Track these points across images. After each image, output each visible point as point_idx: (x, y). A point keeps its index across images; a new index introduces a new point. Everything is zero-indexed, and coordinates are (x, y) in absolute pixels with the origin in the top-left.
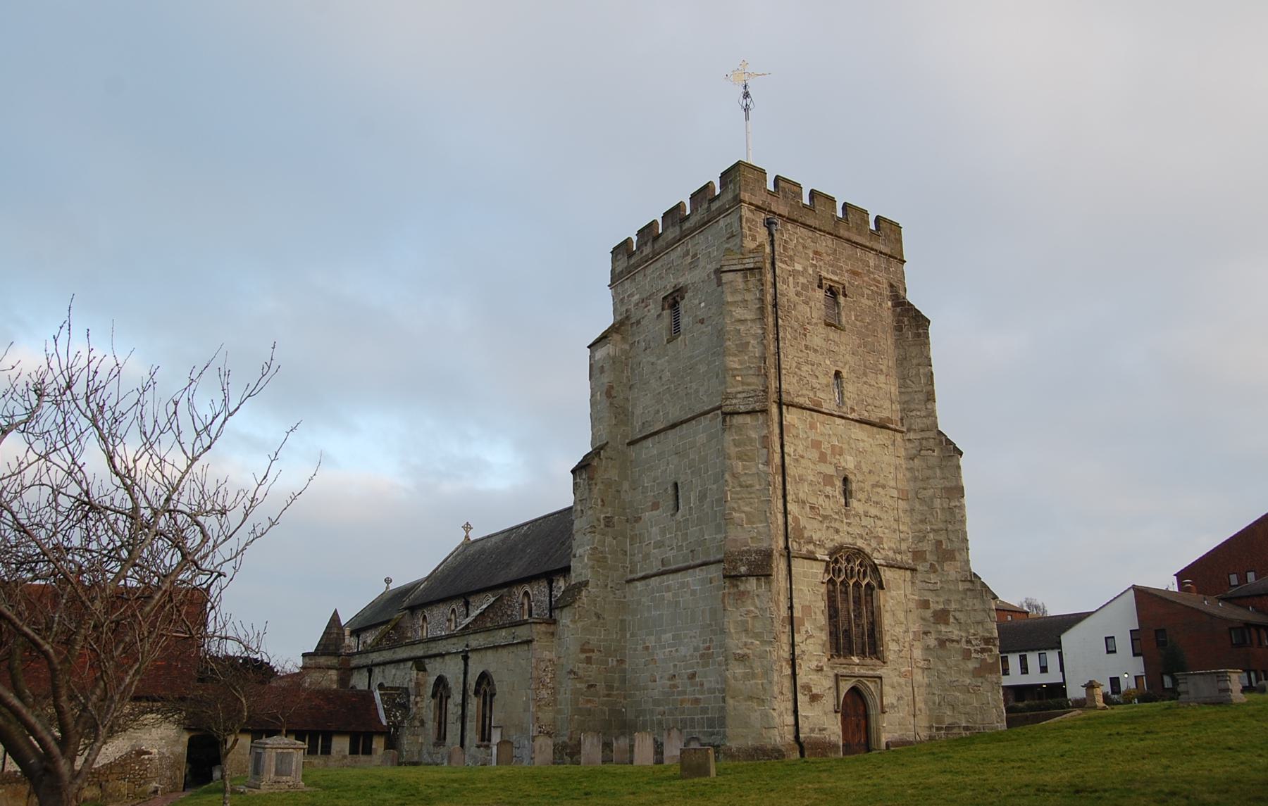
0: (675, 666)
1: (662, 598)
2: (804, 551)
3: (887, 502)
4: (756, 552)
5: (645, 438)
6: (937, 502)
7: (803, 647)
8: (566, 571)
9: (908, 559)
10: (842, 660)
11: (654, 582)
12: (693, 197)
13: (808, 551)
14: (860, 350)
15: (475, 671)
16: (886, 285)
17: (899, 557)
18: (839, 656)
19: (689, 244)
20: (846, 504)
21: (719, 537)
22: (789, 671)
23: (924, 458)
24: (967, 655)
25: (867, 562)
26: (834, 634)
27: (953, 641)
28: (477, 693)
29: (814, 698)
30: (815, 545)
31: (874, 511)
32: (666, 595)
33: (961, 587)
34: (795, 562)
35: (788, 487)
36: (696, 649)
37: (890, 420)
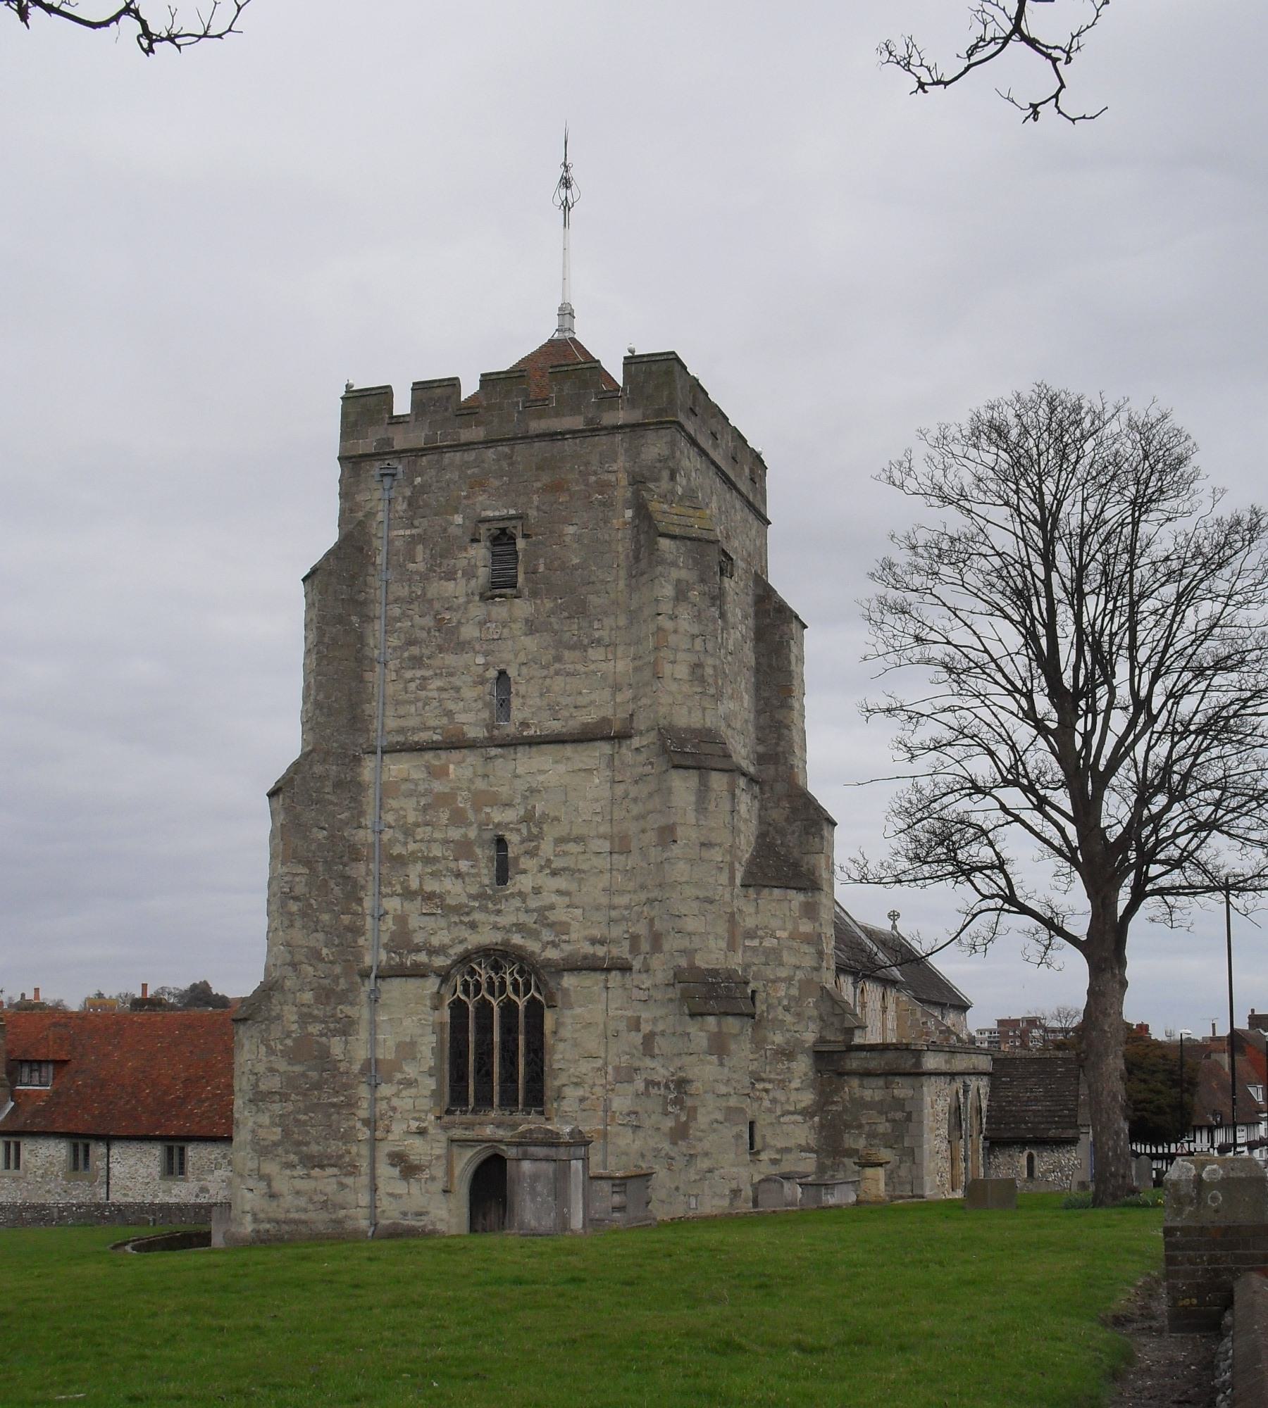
17: (601, 951)
37: (605, 720)
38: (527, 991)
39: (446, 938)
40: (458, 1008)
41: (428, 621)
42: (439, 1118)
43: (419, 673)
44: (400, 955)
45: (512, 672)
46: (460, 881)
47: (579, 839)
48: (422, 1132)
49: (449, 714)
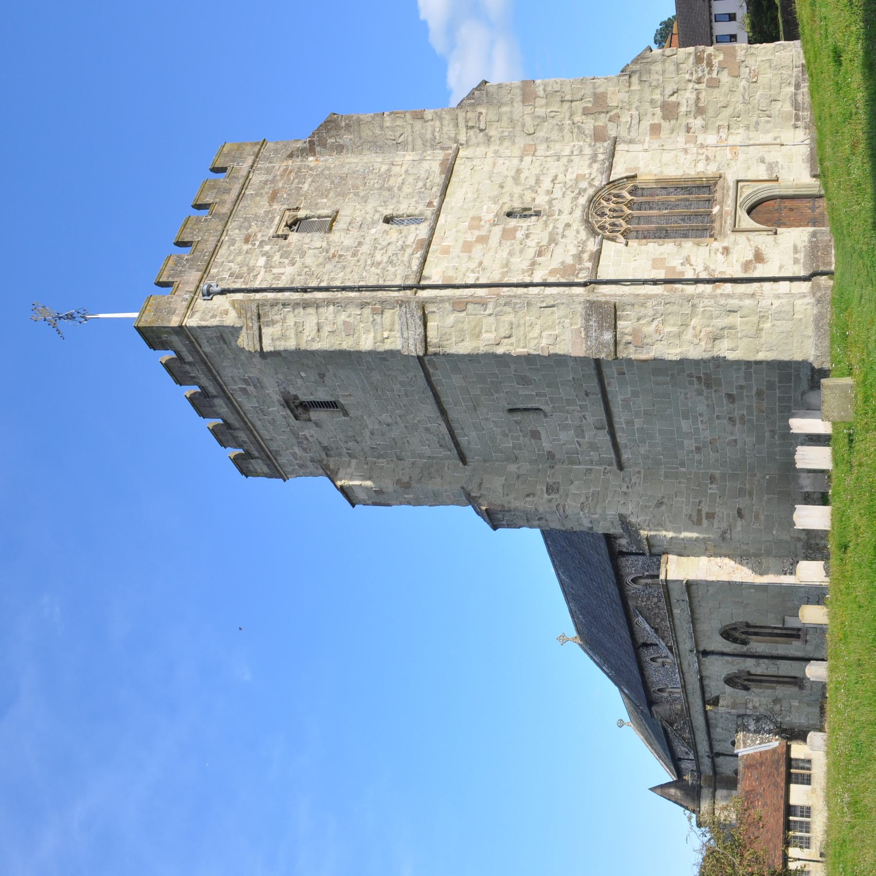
0: (718, 417)
1: (641, 430)
2: (589, 265)
3: (536, 170)
4: (587, 320)
5: (457, 445)
6: (541, 111)
7: (700, 268)
8: (609, 538)
9: (603, 148)
10: (716, 225)
11: (622, 439)
12: (179, 382)
13: (590, 260)
14: (362, 194)
15: (719, 644)
16: (290, 162)
17: (601, 157)
18: (712, 228)
19: (233, 387)
20: (538, 214)
21: (571, 364)
22: (728, 286)
23: (489, 123)
24: (714, 84)
25: (604, 193)
27: (698, 99)
28: (744, 643)
29: (759, 257)
30: (582, 252)
31: (546, 184)
32: (637, 426)
33: (635, 87)
34: (602, 275)
35: (514, 280)
36: (700, 393)
42: (716, 239)
44: (581, 270)
45: (388, 212)
46: (531, 235)
47: (519, 171)
48: (726, 250)
49: (403, 248)
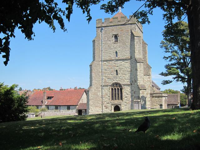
26: (112, 97)
37: (128, 57)
38: (120, 87)
39: (111, 82)
40: (112, 89)
41: (107, 46)
43: (107, 52)
